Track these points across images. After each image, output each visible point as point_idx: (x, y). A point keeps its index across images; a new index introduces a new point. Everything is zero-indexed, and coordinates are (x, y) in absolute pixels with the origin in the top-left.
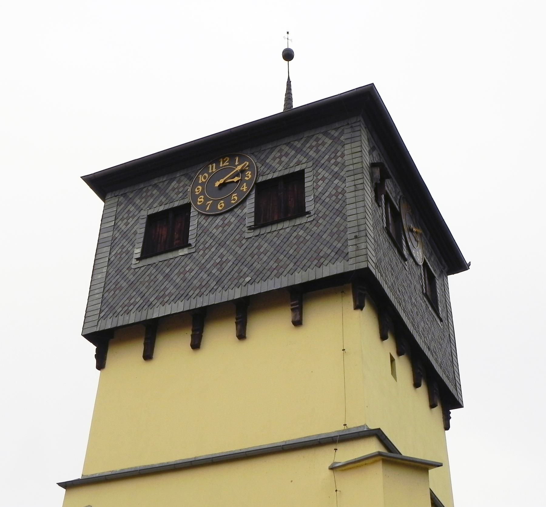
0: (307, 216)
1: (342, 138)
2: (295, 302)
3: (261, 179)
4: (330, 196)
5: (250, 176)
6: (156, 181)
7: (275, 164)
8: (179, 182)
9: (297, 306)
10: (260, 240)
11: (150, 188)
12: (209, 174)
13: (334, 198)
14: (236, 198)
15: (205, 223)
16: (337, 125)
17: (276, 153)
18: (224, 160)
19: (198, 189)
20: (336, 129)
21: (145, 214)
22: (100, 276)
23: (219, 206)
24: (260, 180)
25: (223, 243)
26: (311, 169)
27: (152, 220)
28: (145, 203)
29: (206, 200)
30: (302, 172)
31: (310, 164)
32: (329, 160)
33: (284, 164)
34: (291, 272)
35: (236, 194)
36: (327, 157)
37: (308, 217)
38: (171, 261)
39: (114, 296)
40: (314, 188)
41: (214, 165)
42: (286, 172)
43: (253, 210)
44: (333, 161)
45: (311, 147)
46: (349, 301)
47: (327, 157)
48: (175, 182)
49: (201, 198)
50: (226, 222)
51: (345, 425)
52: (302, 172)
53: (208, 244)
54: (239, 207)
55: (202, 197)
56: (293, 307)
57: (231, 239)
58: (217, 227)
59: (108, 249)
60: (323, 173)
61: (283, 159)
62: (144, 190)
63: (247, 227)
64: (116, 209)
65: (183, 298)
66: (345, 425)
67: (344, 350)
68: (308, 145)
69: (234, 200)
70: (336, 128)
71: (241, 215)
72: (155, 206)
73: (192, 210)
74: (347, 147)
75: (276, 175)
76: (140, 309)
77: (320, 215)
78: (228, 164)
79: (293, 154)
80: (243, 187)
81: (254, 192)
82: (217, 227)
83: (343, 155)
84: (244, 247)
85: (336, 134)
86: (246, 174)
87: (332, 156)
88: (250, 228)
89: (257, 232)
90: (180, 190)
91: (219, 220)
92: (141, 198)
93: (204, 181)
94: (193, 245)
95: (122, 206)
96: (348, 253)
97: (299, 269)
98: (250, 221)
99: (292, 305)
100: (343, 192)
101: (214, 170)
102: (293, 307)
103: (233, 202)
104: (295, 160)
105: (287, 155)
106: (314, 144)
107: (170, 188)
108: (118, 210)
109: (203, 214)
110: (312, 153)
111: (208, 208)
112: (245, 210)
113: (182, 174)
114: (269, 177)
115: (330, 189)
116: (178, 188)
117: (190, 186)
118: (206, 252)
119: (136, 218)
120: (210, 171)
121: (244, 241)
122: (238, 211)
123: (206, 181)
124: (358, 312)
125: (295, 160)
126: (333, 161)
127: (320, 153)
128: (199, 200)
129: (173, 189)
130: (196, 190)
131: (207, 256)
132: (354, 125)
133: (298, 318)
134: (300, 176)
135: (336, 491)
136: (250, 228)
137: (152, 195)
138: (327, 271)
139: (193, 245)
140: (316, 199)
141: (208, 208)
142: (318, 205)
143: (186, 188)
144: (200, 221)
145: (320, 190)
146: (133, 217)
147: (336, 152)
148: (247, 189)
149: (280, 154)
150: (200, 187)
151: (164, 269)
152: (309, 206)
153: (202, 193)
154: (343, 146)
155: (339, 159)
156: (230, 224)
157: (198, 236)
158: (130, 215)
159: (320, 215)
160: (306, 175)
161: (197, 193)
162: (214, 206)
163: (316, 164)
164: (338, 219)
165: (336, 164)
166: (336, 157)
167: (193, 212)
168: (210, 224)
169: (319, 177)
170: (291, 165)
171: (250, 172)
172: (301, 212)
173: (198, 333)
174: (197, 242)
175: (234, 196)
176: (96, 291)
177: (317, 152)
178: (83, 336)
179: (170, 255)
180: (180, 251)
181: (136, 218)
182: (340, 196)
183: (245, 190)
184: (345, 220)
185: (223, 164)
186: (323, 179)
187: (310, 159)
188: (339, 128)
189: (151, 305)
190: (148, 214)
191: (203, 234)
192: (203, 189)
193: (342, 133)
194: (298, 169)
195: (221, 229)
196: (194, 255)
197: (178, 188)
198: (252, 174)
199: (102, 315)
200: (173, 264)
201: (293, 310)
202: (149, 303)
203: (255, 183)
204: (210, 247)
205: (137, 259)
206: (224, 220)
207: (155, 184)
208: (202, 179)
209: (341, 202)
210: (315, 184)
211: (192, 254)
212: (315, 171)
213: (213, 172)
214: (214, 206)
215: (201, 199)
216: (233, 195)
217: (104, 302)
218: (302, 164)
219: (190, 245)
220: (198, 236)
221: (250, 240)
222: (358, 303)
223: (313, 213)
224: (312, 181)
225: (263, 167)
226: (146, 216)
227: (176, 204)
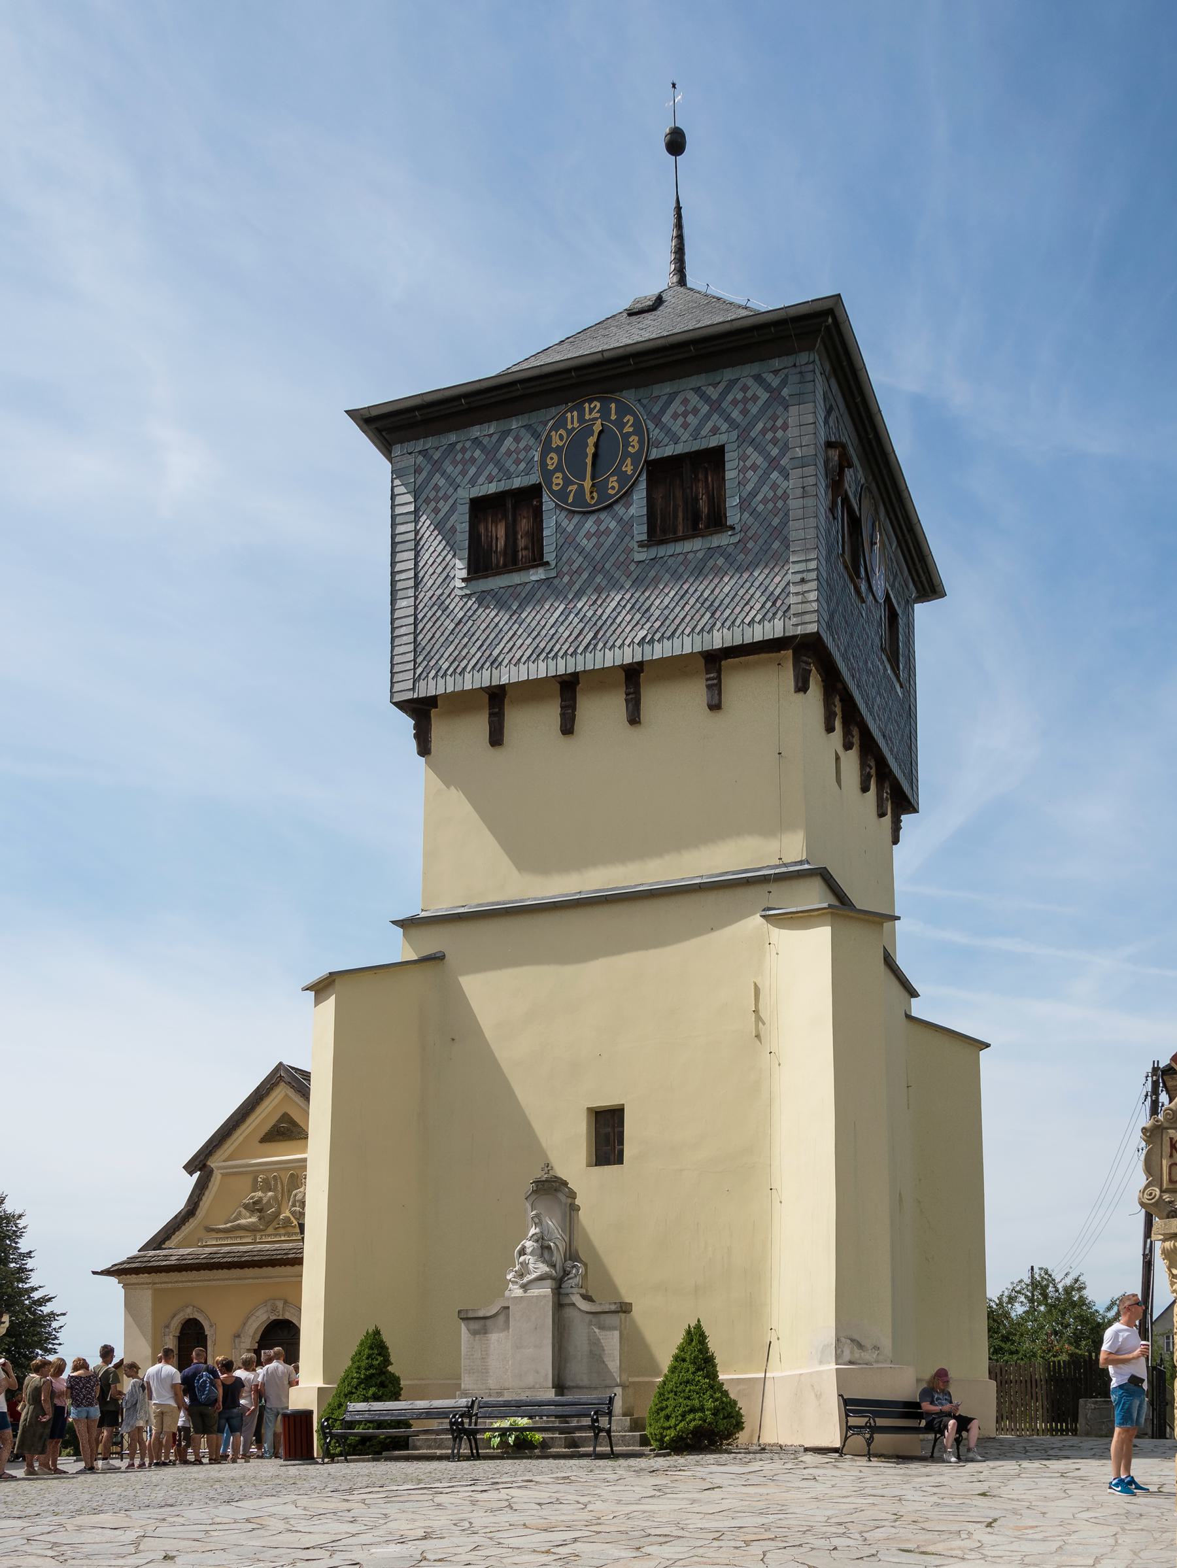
0: (730, 533)
1: (785, 392)
2: (712, 675)
3: (655, 454)
4: (765, 501)
5: (637, 447)
6: (476, 431)
7: (676, 427)
8: (517, 439)
9: (715, 681)
10: (657, 566)
11: (468, 444)
12: (569, 432)
13: (770, 505)
14: (616, 485)
15: (570, 525)
16: (776, 363)
17: (676, 406)
18: (592, 406)
20: (776, 372)
21: (467, 493)
22: (404, 603)
24: (652, 457)
25: (600, 566)
26: (736, 445)
27: (480, 507)
28: (464, 473)
30: (720, 451)
31: (734, 434)
32: (764, 432)
33: (691, 428)
34: (707, 628)
35: (615, 478)
36: (760, 426)
37: (731, 535)
38: (519, 589)
39: (433, 642)
40: (739, 483)
41: (575, 413)
42: (696, 446)
43: (644, 511)
44: (769, 435)
45: (735, 403)
46: (788, 677)
47: (760, 426)
48: (510, 439)
49: (557, 478)
50: (602, 528)
51: (780, 859)
52: (720, 451)
53: (575, 566)
54: (622, 502)
55: (560, 475)
56: (710, 682)
57: (612, 559)
58: (588, 536)
59: (411, 555)
60: (755, 457)
61: (690, 418)
62: (459, 447)
63: (637, 542)
64: (413, 480)
65: (544, 654)
66: (780, 859)
67: (780, 754)
68: (730, 398)
69: (613, 488)
70: (775, 371)
71: (626, 518)
72: (480, 481)
73: (545, 498)
74: (793, 410)
75: (680, 449)
76: (478, 668)
77: (750, 534)
79: (705, 412)
80: (626, 466)
81: (644, 476)
82: (588, 536)
83: (785, 427)
84: (634, 576)
85: (775, 382)
86: (630, 440)
87: (769, 426)
88: (641, 544)
89: (653, 552)
90: (521, 457)
91: (590, 524)
92: (455, 463)
94: (553, 564)
95: (424, 474)
96: (790, 605)
97: (719, 624)
98: (640, 531)
99: (707, 680)
100: (785, 497)
101: (576, 425)
102: (710, 682)
103: (611, 492)
104: (710, 425)
105: (695, 411)
106: (740, 396)
107: (503, 450)
108: (419, 482)
109: (563, 509)
110: (735, 414)
112: (632, 510)
113: (520, 424)
114: (669, 451)
115: (765, 488)
116: (517, 451)
117: (536, 451)
118: (574, 578)
119: (451, 501)
120: (569, 427)
121: (632, 567)
122: (619, 509)
123: (564, 445)
124: (801, 694)
125: (710, 425)
126: (769, 435)
127: (749, 416)
128: (555, 481)
129: (509, 453)
130: (549, 461)
131: (577, 586)
132: (804, 369)
133: (715, 702)
134: (714, 458)
135: (770, 944)
136: (641, 544)
137: (473, 460)
138: (759, 633)
139: (553, 564)
140: (744, 505)
142: (746, 515)
143: (530, 455)
144: (559, 520)
145: (749, 487)
146: (446, 498)
147: (775, 418)
148: (634, 470)
149: (684, 408)
150: (553, 455)
151: (509, 602)
152: (733, 517)
153: (559, 468)
154: (786, 408)
155: (780, 434)
156: (607, 532)
157: (559, 549)
158: (440, 494)
159: (750, 534)
160: (727, 457)
161: (551, 468)
163: (744, 438)
164: (776, 545)
165: (775, 442)
166: (774, 429)
167: (548, 502)
168: (578, 527)
169: (749, 463)
170: (704, 433)
171: (636, 438)
172: (717, 522)
173: (570, 711)
174: (558, 558)
175: (612, 482)
176: (403, 631)
177: (745, 412)
178: (396, 704)
179: (516, 578)
180: (532, 571)
181: (451, 501)
182: (780, 504)
183: (629, 473)
184: (788, 547)
185: (590, 414)
186: (754, 467)
187: (734, 425)
188: (780, 370)
189: (495, 663)
190: (471, 497)
191: (566, 546)
192: (560, 460)
193: (784, 383)
194: (713, 442)
195: (594, 539)
196: (556, 582)
197: (517, 451)
198: (641, 442)
199: (419, 671)
200: (523, 595)
201: (708, 687)
202: (492, 659)
203: (645, 461)
204: (579, 571)
205: (463, 580)
206: (598, 522)
207: (477, 438)
208: (556, 442)
209: (781, 514)
210: (741, 476)
211: (551, 580)
212: (741, 453)
213: (573, 429)
215: (558, 480)
216: (611, 479)
217: (419, 650)
218: (720, 434)
219: (547, 563)
220: (558, 548)
221: (642, 566)
222: (800, 685)
223: (738, 528)
224: (737, 470)
225: (657, 430)
226: (468, 501)
227: (517, 483)
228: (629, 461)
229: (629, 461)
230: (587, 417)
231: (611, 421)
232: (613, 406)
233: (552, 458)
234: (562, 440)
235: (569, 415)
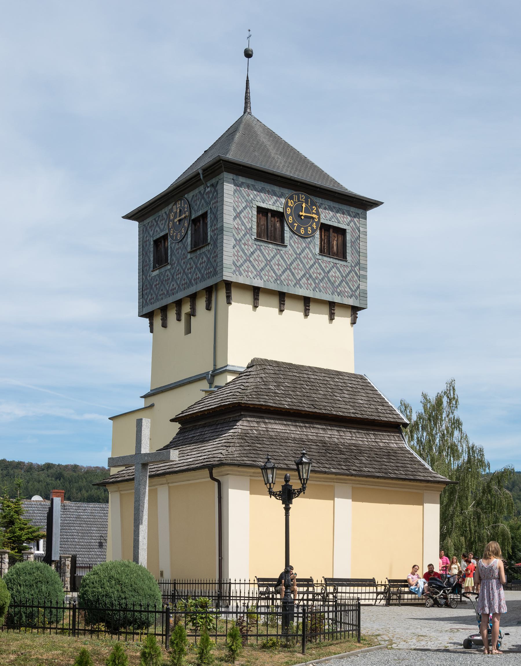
12: (295, 202)
19: (288, 210)
23: (301, 231)
29: (294, 222)
69: (310, 232)
78: (304, 201)
93: (292, 206)
101: (297, 201)
111: (295, 229)
120: (295, 200)
141: (295, 229)
150: (288, 208)
162: (299, 228)
214: (299, 228)
216: (309, 228)
228: (315, 223)
229: (315, 223)
230: (301, 200)
231: (308, 205)
232: (309, 200)
233: (288, 210)
234: (292, 204)
235: (294, 195)
